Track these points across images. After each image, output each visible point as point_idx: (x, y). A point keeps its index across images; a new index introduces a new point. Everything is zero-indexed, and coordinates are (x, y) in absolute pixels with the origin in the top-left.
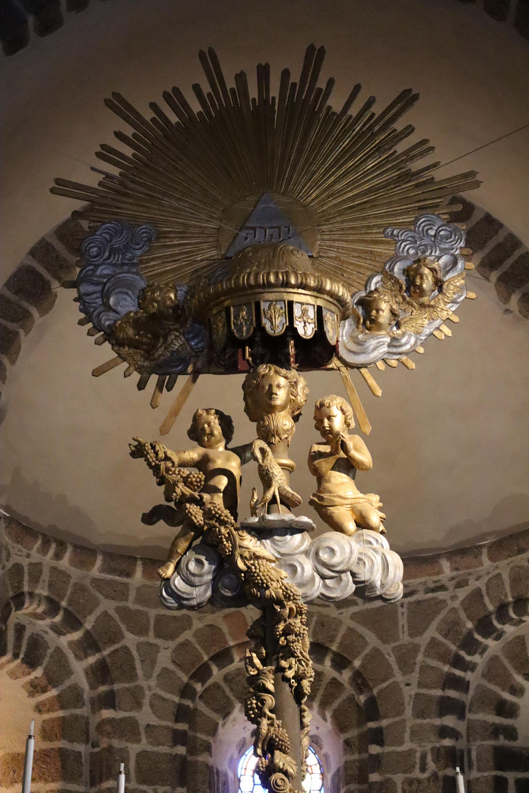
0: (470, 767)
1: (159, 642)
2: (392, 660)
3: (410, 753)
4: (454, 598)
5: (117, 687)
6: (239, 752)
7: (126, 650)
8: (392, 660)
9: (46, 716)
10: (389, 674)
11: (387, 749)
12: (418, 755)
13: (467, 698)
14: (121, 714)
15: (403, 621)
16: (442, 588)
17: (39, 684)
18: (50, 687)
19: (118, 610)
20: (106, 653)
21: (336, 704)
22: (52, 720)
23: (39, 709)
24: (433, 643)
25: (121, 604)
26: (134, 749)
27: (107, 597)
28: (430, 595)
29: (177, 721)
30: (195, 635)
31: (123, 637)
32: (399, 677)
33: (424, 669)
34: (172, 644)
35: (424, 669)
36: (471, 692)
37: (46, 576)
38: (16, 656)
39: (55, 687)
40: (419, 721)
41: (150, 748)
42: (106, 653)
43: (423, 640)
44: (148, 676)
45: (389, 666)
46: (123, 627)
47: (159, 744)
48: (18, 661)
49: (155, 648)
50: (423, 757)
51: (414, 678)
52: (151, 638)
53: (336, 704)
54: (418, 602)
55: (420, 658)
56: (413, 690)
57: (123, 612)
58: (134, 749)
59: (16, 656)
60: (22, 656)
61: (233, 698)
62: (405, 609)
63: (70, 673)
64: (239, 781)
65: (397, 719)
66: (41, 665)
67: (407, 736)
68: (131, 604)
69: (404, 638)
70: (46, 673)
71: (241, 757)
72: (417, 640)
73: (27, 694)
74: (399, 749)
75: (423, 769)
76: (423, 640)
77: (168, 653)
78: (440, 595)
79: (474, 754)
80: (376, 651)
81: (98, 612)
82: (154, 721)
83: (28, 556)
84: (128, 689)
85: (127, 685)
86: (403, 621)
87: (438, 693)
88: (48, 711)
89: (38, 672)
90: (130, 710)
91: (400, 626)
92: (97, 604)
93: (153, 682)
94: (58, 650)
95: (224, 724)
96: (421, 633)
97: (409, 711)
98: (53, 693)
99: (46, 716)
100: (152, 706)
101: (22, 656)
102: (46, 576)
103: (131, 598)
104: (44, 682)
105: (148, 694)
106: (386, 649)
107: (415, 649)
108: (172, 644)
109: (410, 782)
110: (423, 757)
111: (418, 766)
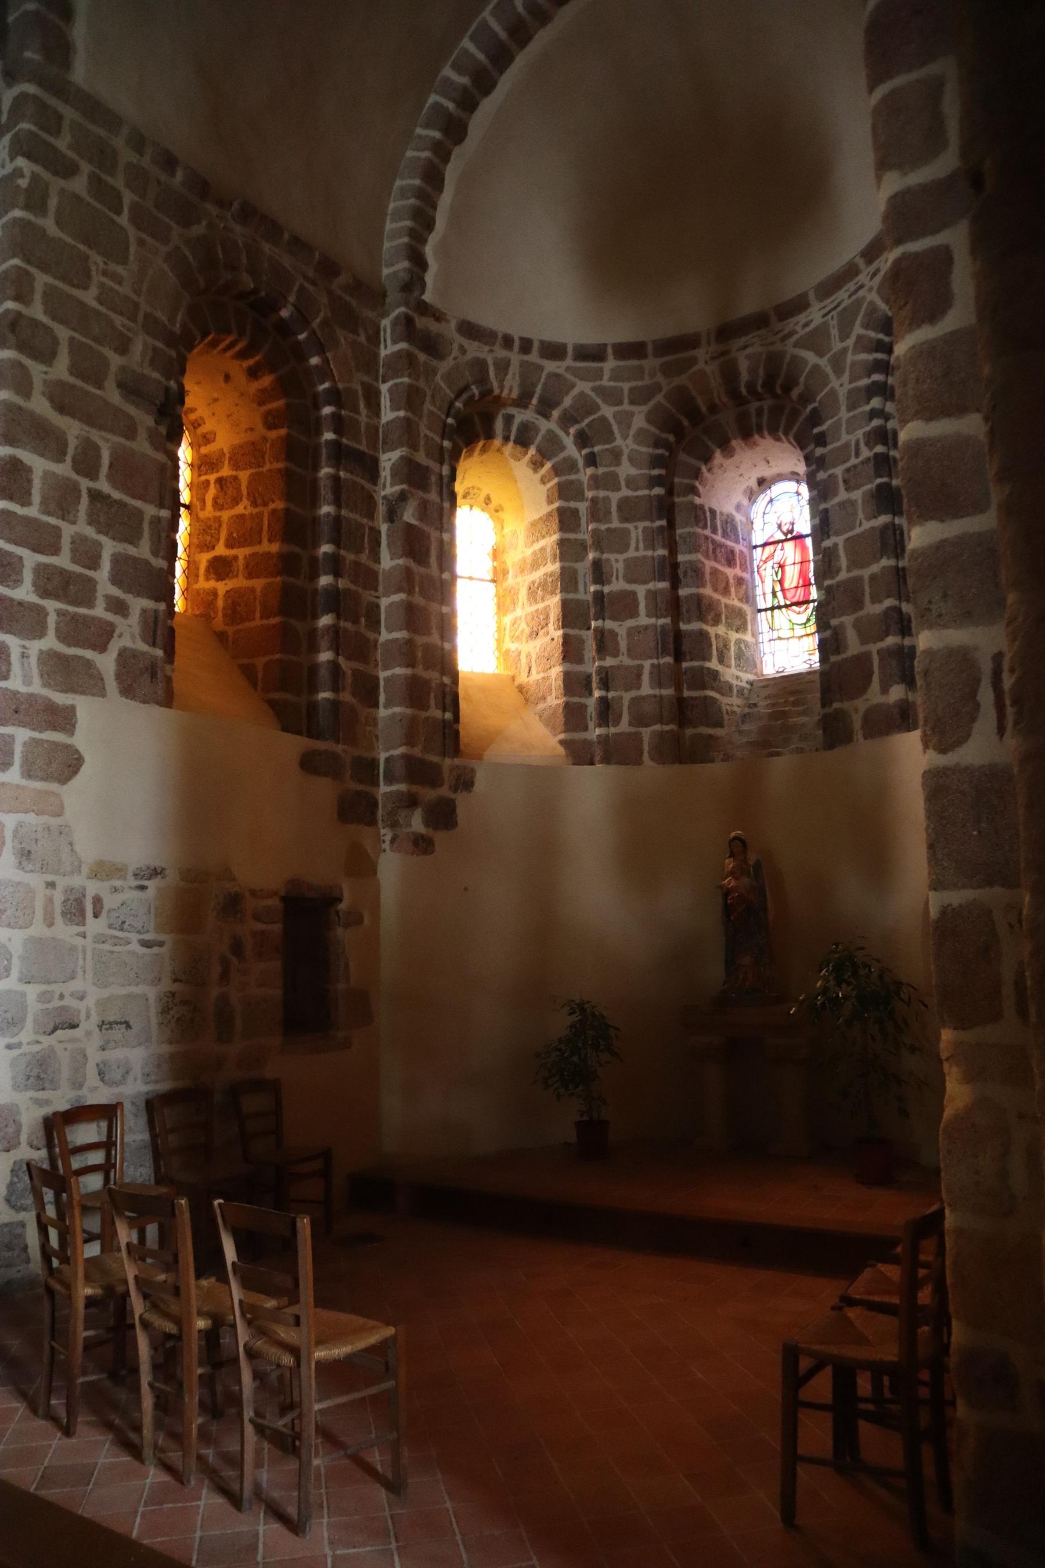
1: (633, 408)
2: (829, 370)
3: (847, 445)
5: (597, 449)
6: (750, 499)
7: (604, 419)
8: (829, 370)
9: (549, 485)
11: (830, 447)
12: (853, 443)
14: (601, 470)
15: (834, 332)
16: (861, 287)
17: (536, 461)
18: (545, 461)
19: (594, 389)
20: (584, 424)
21: (795, 429)
22: (552, 488)
23: (543, 481)
24: (860, 337)
25: (597, 383)
26: (615, 497)
27: (582, 380)
28: (854, 298)
29: (654, 468)
30: (665, 397)
31: (599, 409)
34: (645, 408)
37: (514, 368)
38: (506, 439)
39: (548, 460)
40: (851, 414)
41: (630, 493)
42: (584, 424)
43: (850, 342)
44: (625, 437)
45: (827, 375)
46: (599, 401)
47: (637, 489)
48: (511, 444)
49: (632, 414)
50: (857, 444)
51: (846, 376)
52: (626, 406)
53: (795, 429)
54: (845, 309)
55: (850, 358)
56: (847, 387)
57: (600, 391)
58: (615, 497)
59: (506, 439)
60: (512, 438)
61: (710, 443)
62: (835, 322)
63: (563, 448)
64: (752, 523)
65: (835, 418)
66: (532, 444)
68: (606, 382)
69: (837, 346)
70: (539, 450)
71: (753, 504)
73: (531, 472)
74: (838, 444)
76: (850, 342)
77: (642, 416)
78: (861, 293)
80: (816, 367)
81: (575, 392)
82: (633, 471)
83: (491, 351)
84: (607, 450)
85: (607, 446)
86: (834, 332)
87: (865, 382)
88: (549, 481)
89: (532, 451)
90: (610, 466)
91: (832, 337)
92: (573, 386)
93: (630, 441)
94: (550, 432)
95: (709, 470)
96: (848, 337)
97: (843, 408)
98: (548, 465)
99: (549, 485)
100: (631, 460)
101: (512, 438)
102: (514, 368)
103: (606, 377)
104: (539, 458)
105: (626, 452)
106: (823, 362)
107: (845, 350)
108: (645, 408)
110: (857, 444)
111: (853, 454)
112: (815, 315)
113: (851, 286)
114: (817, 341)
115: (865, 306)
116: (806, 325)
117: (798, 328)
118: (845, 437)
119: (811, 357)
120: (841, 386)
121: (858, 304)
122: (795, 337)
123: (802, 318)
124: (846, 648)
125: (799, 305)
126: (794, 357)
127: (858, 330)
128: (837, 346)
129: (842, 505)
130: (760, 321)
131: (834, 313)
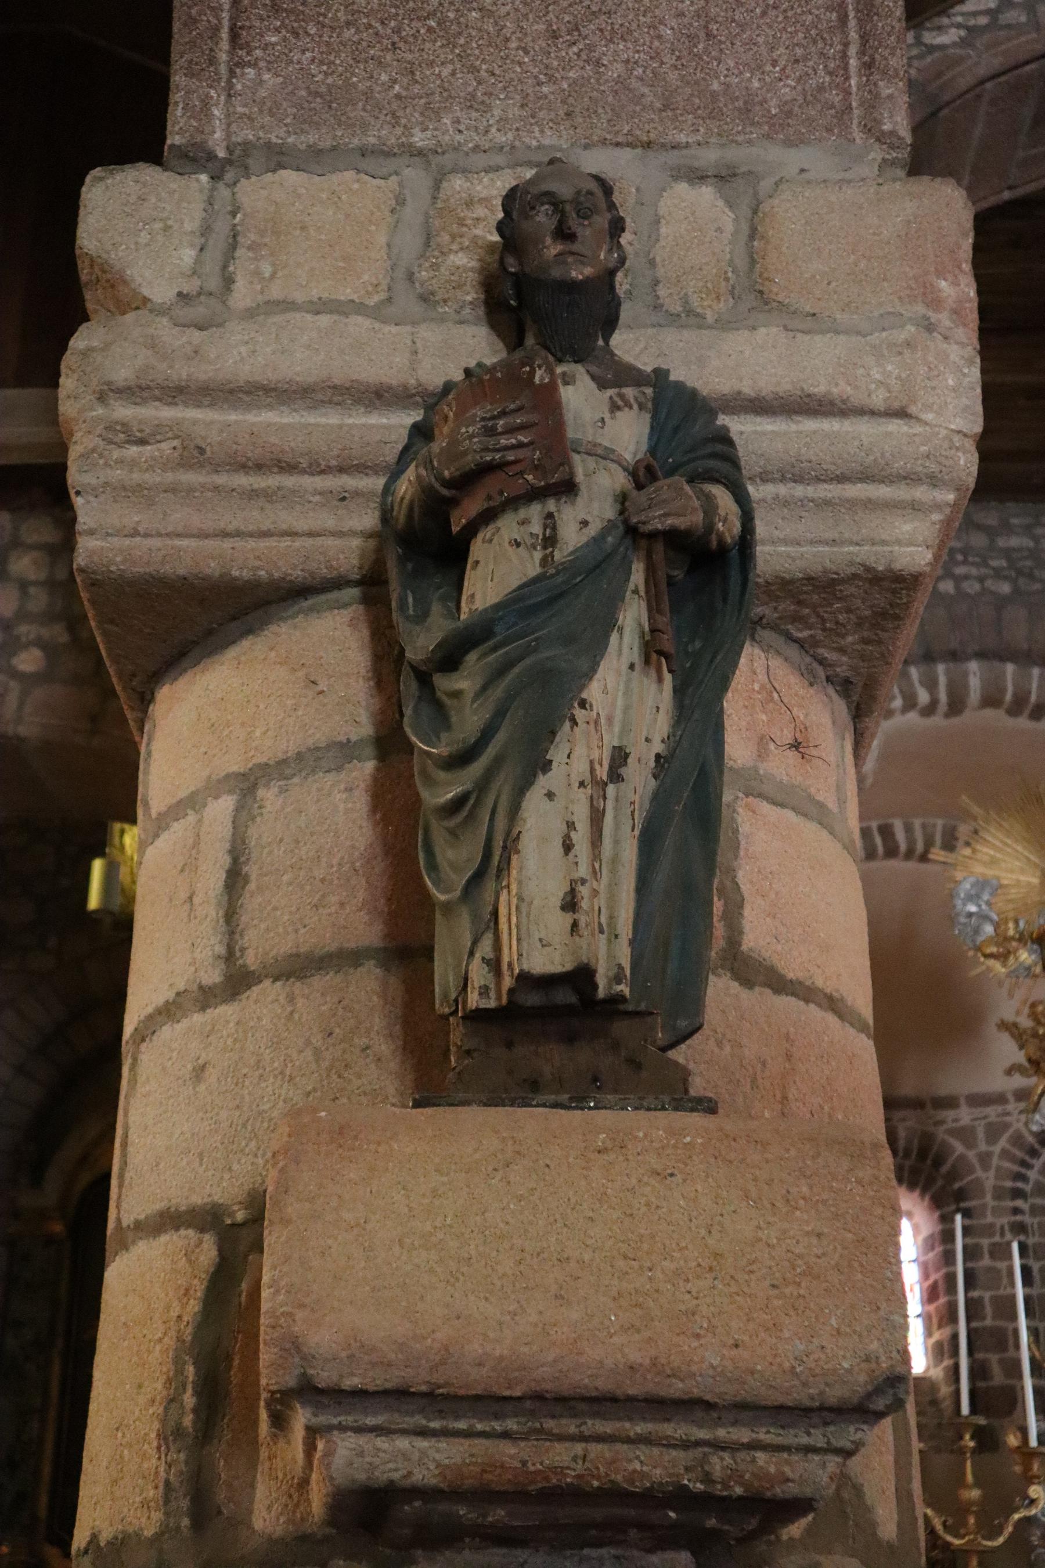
0: (1034, 1235)
2: (975, 1161)
3: (992, 1226)
4: (1018, 1121)
8: (975, 1161)
10: (972, 1171)
13: (1028, 1188)
15: (981, 1134)
16: (1008, 1114)
21: (933, 1190)
32: (979, 1173)
33: (999, 1169)
35: (999, 1169)
36: (1031, 1183)
43: (997, 1149)
50: (1002, 1228)
51: (992, 1174)
67: (989, 1212)
72: (991, 1149)
75: (1002, 1234)
76: (997, 1149)
78: (1008, 1119)
79: (1036, 1226)
80: (962, 1157)
86: (981, 1134)
87: (1009, 1184)
106: (971, 1155)
109: (994, 1245)
110: (1002, 1228)
112: (964, 1115)
113: (1000, 1109)
114: (966, 1135)
115: (1011, 1131)
116: (955, 1120)
117: (950, 1119)
118: (989, 1219)
119: (959, 1148)
120: (989, 1179)
121: (1006, 1126)
122: (945, 1127)
123: (950, 1114)
124: (992, 1378)
125: (950, 1103)
126: (943, 1141)
127: (1003, 1142)
128: (983, 1147)
129: (990, 1270)
130: (918, 1104)
131: (983, 1122)
